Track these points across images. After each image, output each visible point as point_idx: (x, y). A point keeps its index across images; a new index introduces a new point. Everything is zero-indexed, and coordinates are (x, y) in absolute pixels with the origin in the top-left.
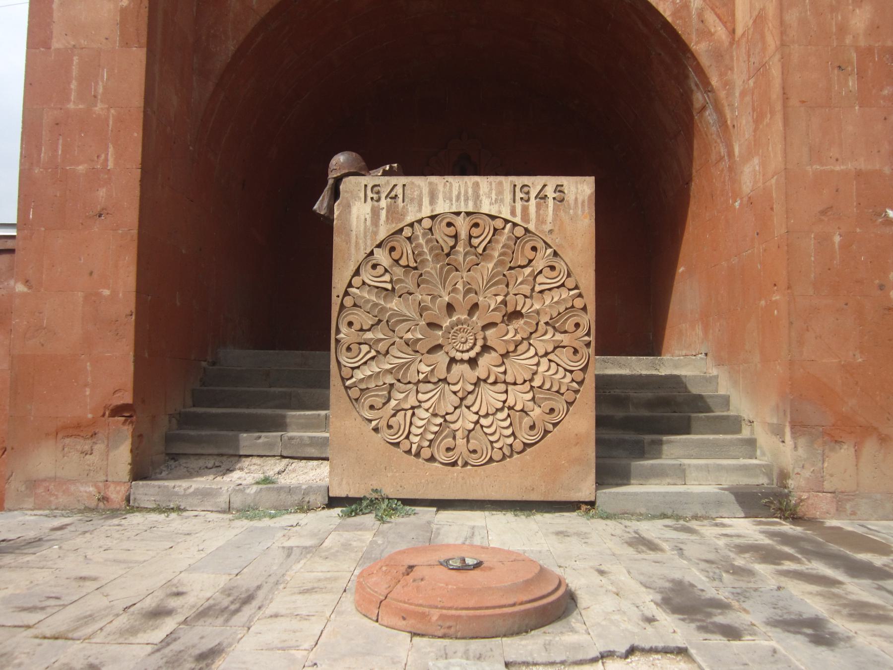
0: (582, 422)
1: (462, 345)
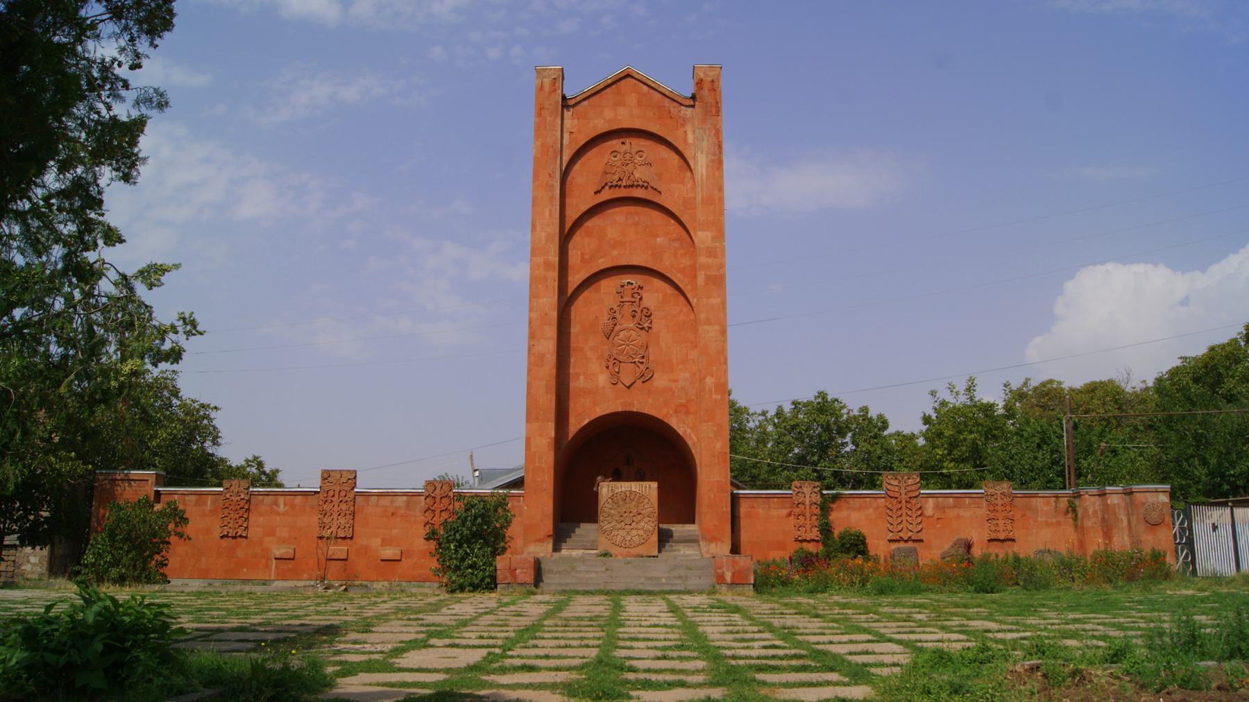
0: (655, 538)
1: (628, 521)
